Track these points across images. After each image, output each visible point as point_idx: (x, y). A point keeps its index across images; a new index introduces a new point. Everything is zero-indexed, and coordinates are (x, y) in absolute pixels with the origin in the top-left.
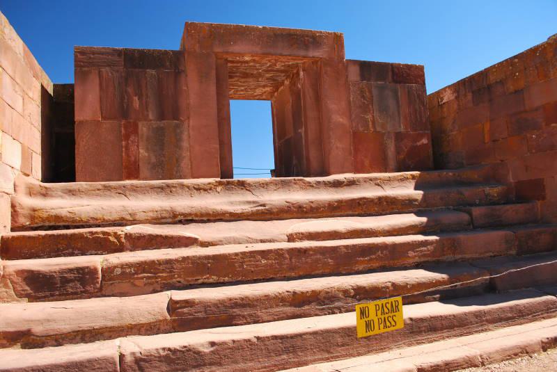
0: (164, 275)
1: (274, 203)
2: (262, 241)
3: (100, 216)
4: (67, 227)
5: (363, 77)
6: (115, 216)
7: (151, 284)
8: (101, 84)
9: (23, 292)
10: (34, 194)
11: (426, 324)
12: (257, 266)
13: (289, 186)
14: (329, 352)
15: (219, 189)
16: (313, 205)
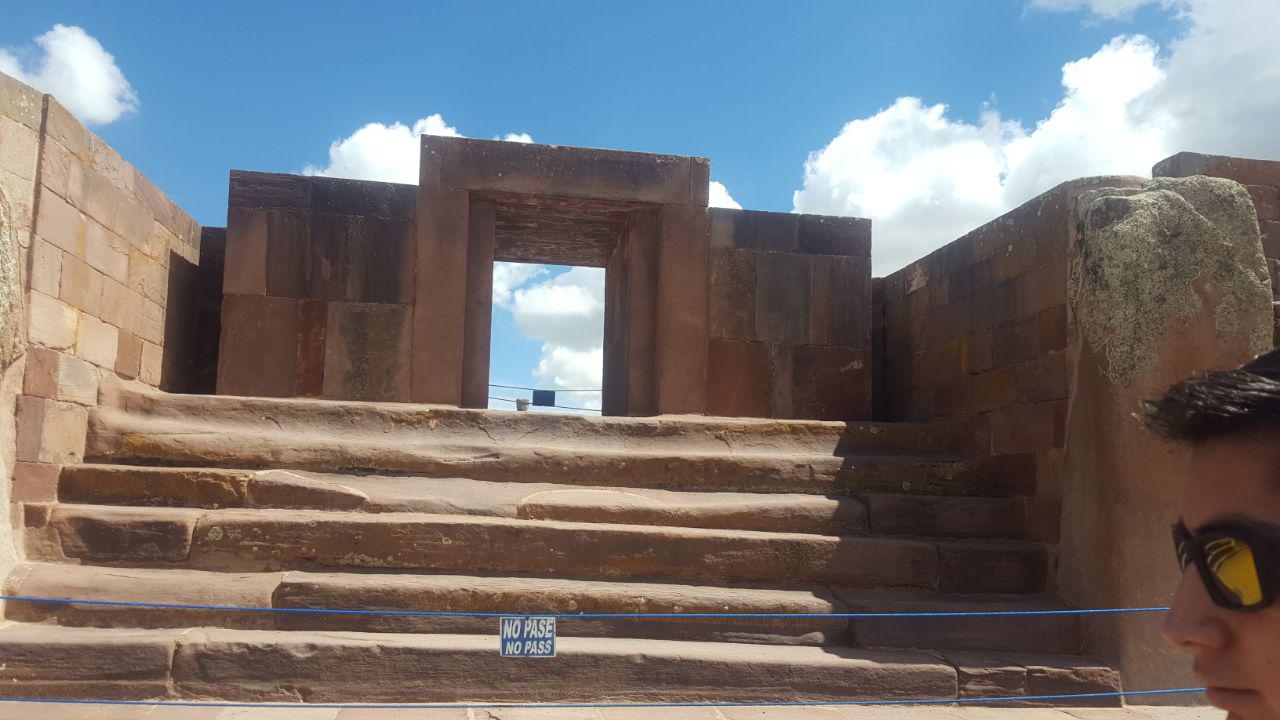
0: (285, 546)
1: (513, 453)
2: (471, 512)
3: (223, 450)
4: (170, 464)
6: (247, 453)
7: (264, 558)
8: (270, 236)
9: (73, 549)
10: (132, 408)
11: (669, 670)
12: (435, 547)
13: (555, 427)
14: (491, 686)
15: (433, 423)
16: (581, 464)
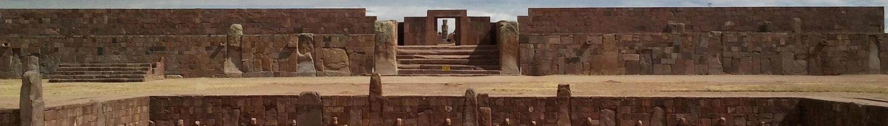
5: (471, 21)
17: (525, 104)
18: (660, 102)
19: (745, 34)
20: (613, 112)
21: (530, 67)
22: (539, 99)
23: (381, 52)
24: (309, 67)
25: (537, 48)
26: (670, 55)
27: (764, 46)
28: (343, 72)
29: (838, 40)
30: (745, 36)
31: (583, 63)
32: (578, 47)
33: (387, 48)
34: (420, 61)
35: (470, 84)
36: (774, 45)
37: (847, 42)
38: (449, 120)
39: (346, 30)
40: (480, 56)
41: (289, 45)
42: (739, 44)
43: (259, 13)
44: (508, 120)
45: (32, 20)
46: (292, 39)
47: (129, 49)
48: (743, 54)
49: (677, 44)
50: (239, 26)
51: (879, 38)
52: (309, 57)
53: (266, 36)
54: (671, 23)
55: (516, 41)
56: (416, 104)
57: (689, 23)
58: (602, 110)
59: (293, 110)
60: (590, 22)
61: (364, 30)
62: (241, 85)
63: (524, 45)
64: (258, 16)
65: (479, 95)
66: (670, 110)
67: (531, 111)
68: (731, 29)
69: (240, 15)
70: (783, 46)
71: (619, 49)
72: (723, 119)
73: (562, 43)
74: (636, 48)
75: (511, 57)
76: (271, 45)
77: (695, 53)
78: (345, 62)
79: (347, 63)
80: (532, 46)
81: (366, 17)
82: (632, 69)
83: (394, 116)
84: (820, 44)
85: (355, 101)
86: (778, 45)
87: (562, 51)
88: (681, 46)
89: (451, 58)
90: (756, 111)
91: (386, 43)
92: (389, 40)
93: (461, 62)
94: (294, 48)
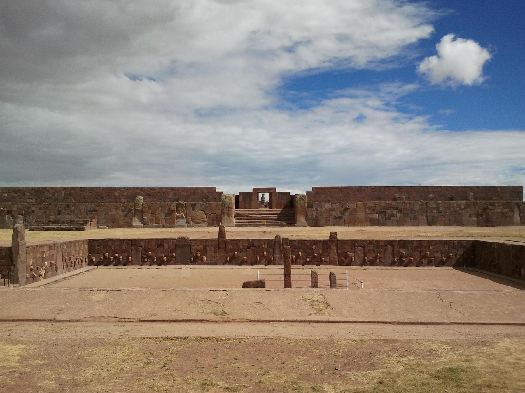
6: (244, 213)
17: (310, 244)
18: (390, 243)
19: (440, 202)
20: (362, 249)
21: (314, 222)
22: (319, 241)
23: (225, 213)
24: (183, 222)
25: (318, 211)
26: (396, 215)
27: (452, 209)
28: (203, 225)
29: (496, 206)
30: (441, 204)
31: (344, 219)
32: (342, 210)
33: (228, 211)
34: (249, 218)
35: (278, 232)
36: (458, 209)
37: (501, 207)
38: (265, 253)
39: (204, 199)
40: (284, 215)
41: (171, 209)
42: (437, 208)
43: (153, 189)
44: (300, 253)
45: (19, 194)
46: (173, 205)
47: (76, 211)
48: (440, 214)
49: (400, 208)
50: (142, 197)
51: (520, 205)
52: (183, 216)
53: (157, 203)
54: (397, 195)
55: (305, 207)
56: (246, 244)
57: (407, 195)
58: (356, 248)
59: (173, 247)
60: (349, 195)
61: (215, 200)
62: (143, 233)
63: (310, 209)
64: (152, 191)
65: (283, 238)
66: (396, 248)
67: (314, 248)
68: (432, 199)
69: (142, 191)
70: (463, 209)
71: (366, 211)
72: (428, 252)
73: (333, 208)
74: (376, 210)
75: (302, 216)
76: (160, 208)
77: (411, 214)
78: (204, 219)
79: (205, 219)
80: (315, 209)
81: (217, 192)
82: (374, 223)
83: (233, 251)
84: (485, 208)
85: (210, 242)
86: (460, 209)
87: (332, 212)
88: (403, 210)
89: (267, 217)
90: (447, 248)
91: (228, 208)
92: (230, 206)
93: (272, 219)
94: (174, 210)
